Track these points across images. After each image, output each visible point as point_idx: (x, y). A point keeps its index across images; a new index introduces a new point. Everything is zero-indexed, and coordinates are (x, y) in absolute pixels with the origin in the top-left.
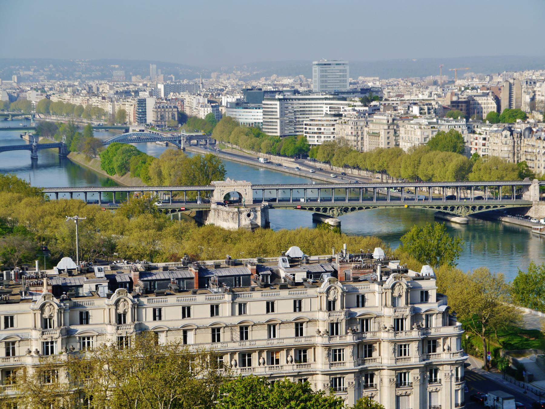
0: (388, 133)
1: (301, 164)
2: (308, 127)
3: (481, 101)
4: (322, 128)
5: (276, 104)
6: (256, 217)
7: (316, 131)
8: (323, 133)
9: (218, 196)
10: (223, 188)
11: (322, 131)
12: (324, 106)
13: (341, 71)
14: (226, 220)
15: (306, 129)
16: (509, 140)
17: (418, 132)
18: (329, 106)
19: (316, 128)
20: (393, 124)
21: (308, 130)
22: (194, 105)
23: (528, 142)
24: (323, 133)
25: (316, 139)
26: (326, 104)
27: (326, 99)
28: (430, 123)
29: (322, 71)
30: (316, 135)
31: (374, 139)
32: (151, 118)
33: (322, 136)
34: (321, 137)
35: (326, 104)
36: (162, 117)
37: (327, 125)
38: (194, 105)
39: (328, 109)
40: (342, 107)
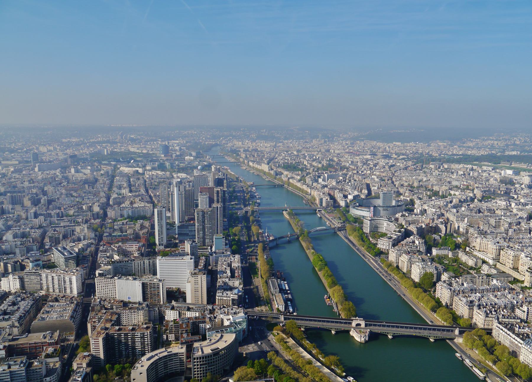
1: (376, 262)
3: (440, 226)
6: (366, 338)
9: (354, 324)
13: (390, 196)
16: (450, 293)
17: (419, 270)
20: (410, 260)
22: (338, 196)
23: (456, 299)
27: (386, 220)
28: (423, 267)
29: (384, 196)
31: (403, 263)
32: (324, 204)
36: (328, 205)
38: (338, 196)
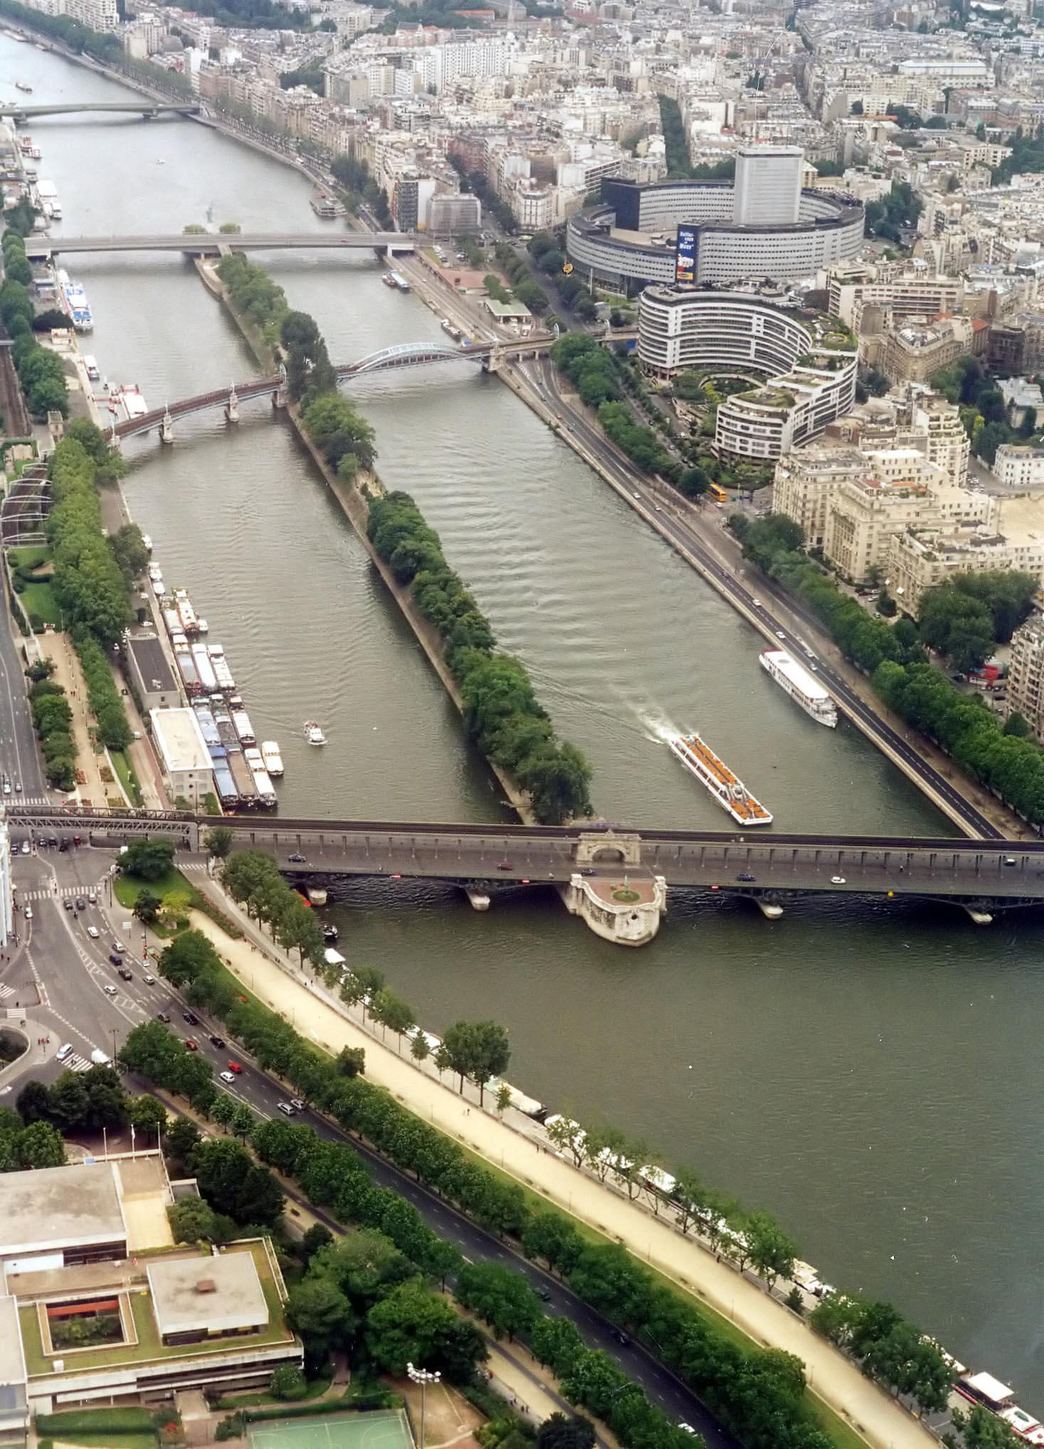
0: (871, 527)
2: (725, 419)
4: (752, 427)
5: (666, 312)
7: (739, 429)
8: (750, 436)
10: (591, 844)
11: (750, 432)
12: (755, 316)
14: (597, 919)
15: (721, 420)
18: (763, 318)
19: (740, 424)
21: (724, 424)
24: (750, 436)
25: (738, 444)
26: (761, 313)
30: (739, 438)
33: (751, 441)
34: (746, 442)
35: (761, 313)
37: (761, 424)
39: (761, 322)
40: (787, 328)
